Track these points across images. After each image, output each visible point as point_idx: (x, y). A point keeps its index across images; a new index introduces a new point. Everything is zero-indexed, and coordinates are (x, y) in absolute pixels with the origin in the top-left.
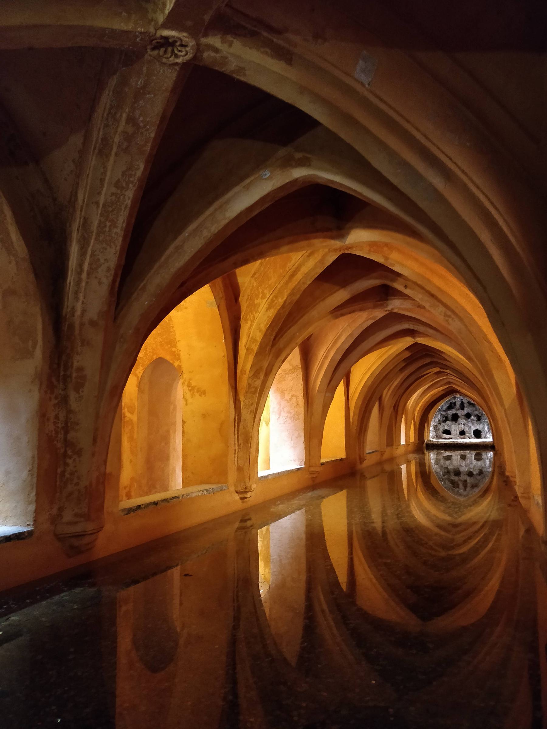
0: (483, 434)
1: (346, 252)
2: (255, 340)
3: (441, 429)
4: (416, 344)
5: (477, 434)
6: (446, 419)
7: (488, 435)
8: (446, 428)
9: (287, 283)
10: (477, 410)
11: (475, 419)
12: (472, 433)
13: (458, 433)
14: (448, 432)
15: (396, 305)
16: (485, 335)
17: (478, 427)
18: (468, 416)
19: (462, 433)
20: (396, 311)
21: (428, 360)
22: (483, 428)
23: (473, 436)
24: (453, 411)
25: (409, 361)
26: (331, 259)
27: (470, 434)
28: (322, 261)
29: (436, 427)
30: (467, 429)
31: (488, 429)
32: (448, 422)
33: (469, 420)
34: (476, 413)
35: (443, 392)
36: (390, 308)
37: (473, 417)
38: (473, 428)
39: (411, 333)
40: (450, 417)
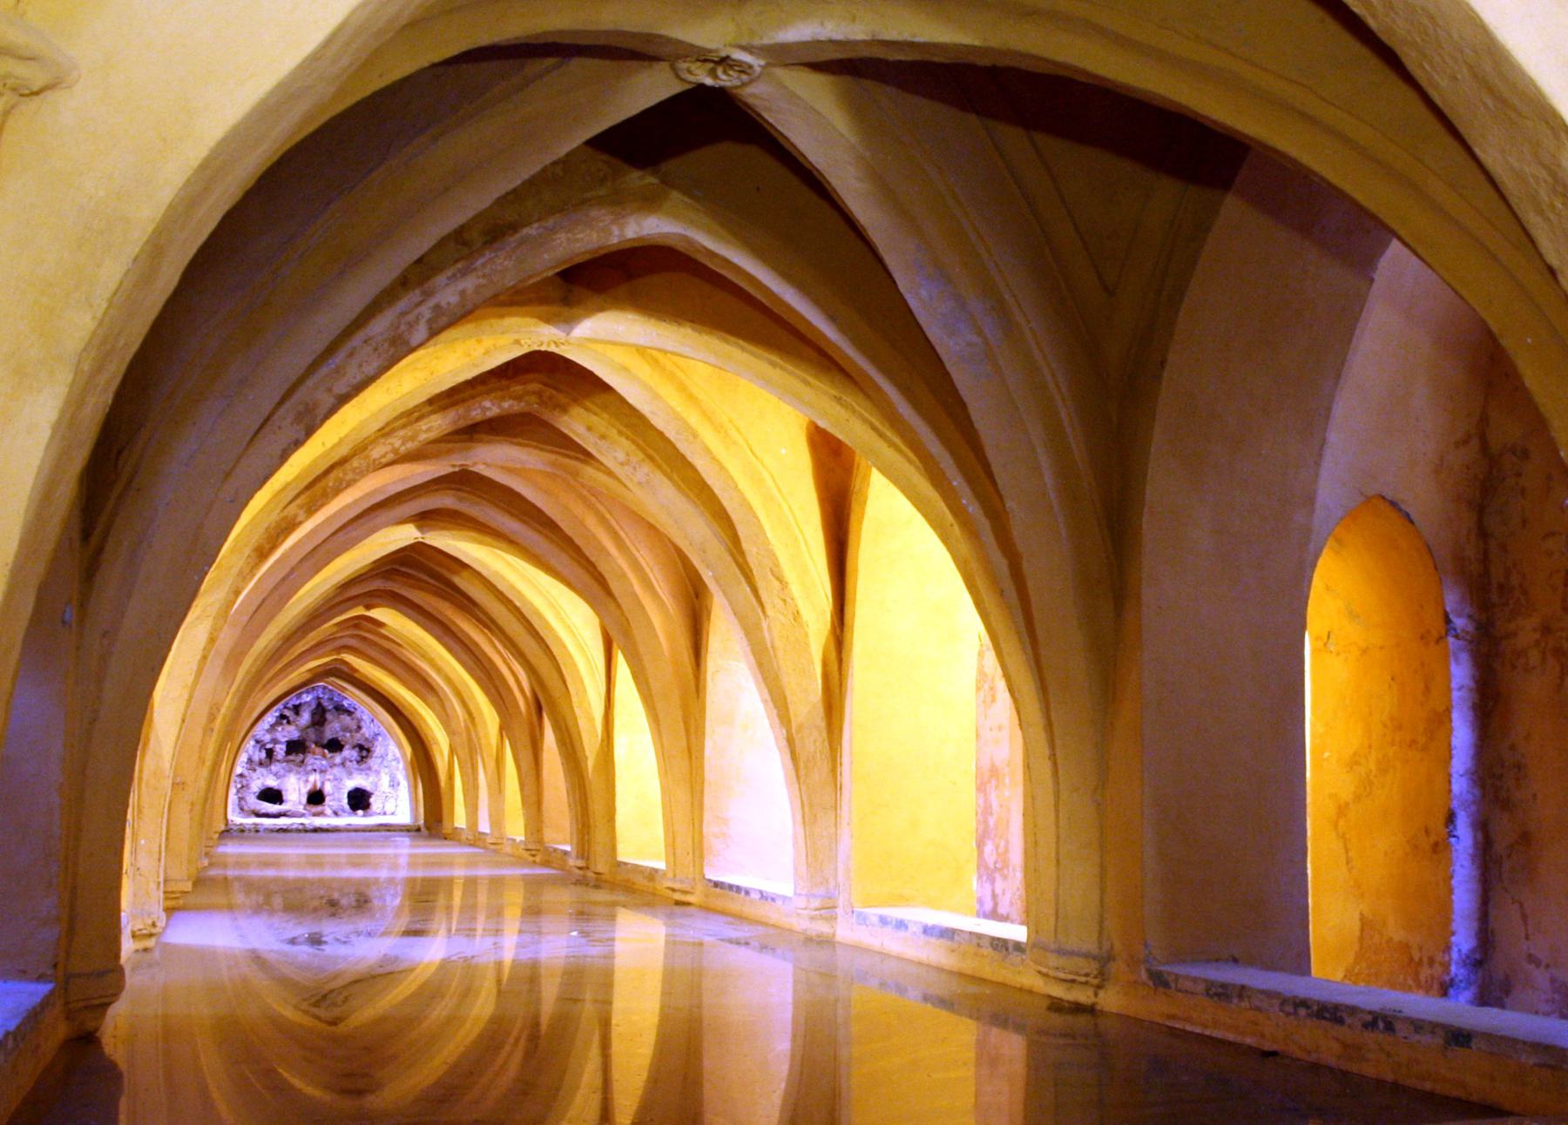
1: (553, 349)
3: (256, 785)
7: (389, 807)
8: (272, 782)
11: (355, 754)
12: (345, 801)
13: (304, 800)
16: (777, 565)
18: (335, 746)
20: (481, 469)
22: (376, 785)
23: (347, 807)
30: (328, 788)
31: (394, 784)
33: (338, 759)
35: (308, 676)
37: (349, 753)
38: (351, 784)
40: (280, 750)
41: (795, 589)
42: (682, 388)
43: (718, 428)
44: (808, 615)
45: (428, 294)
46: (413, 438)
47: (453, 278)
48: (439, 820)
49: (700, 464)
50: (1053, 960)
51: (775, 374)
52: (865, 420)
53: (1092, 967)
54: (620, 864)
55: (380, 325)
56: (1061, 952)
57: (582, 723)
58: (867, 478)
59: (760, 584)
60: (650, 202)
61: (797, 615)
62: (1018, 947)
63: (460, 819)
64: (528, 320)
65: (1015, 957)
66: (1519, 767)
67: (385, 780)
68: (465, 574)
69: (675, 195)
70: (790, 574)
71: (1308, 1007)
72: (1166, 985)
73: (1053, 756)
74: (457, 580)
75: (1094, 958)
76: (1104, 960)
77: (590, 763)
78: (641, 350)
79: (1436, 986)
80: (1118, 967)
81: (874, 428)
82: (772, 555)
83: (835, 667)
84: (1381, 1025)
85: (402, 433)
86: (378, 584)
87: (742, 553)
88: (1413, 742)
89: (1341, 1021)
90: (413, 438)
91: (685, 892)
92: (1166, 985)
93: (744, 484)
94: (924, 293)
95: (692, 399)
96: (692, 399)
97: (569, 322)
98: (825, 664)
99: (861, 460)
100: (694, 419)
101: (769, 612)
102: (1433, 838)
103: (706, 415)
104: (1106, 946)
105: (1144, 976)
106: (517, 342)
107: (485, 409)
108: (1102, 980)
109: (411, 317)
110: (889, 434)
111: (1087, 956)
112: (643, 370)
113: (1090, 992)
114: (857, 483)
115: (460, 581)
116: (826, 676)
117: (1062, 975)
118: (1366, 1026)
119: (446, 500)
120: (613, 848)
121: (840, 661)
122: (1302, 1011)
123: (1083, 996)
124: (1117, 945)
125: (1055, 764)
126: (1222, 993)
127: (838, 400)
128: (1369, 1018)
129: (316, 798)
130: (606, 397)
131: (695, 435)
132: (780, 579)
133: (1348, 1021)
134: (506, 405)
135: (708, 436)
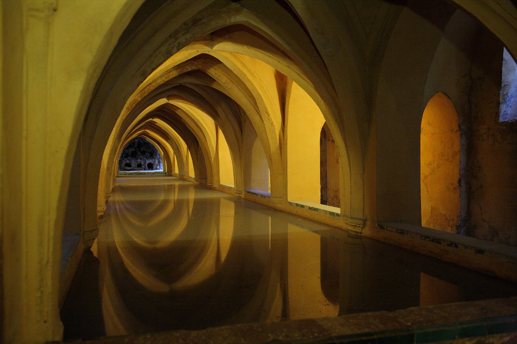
0: (155, 167)
1: (207, 53)
3: (124, 163)
5: (151, 166)
6: (127, 156)
7: (158, 167)
8: (128, 162)
10: (150, 148)
11: (149, 155)
14: (128, 165)
16: (267, 110)
17: (151, 161)
18: (143, 153)
19: (139, 166)
22: (154, 162)
24: (133, 150)
27: (145, 166)
29: (120, 162)
30: (143, 163)
32: (129, 158)
34: (149, 151)
37: (147, 154)
38: (148, 162)
41: (272, 116)
42: (242, 63)
44: (275, 123)
45: (177, 39)
46: (168, 77)
47: (183, 35)
48: (171, 171)
49: (246, 83)
50: (351, 220)
51: (270, 60)
52: (296, 72)
53: (361, 222)
54: (221, 185)
55: (163, 49)
56: (352, 218)
58: (291, 87)
60: (238, 12)
61: (272, 123)
62: (338, 215)
63: (177, 171)
64: (200, 45)
65: (336, 217)
67: (157, 161)
68: (179, 110)
69: (245, 10)
70: (270, 113)
71: (429, 238)
72: (384, 229)
73: (350, 164)
74: (177, 112)
75: (362, 220)
76: (365, 221)
77: (213, 159)
78: (231, 53)
79: (454, 227)
80: (368, 223)
81: (298, 74)
82: (266, 108)
83: (282, 137)
84: (454, 245)
85: (165, 76)
87: (258, 107)
88: (448, 160)
89: (440, 243)
90: (168, 77)
91: (239, 194)
92: (384, 229)
95: (245, 66)
96: (245, 66)
97: (212, 46)
98: (280, 136)
99: (289, 81)
100: (245, 71)
101: (265, 122)
102: (454, 186)
103: (249, 70)
104: (365, 217)
105: (377, 226)
106: (198, 51)
107: (187, 69)
108: (364, 224)
109: (172, 46)
110: (303, 76)
111: (360, 219)
112: (232, 59)
113: (360, 229)
114: (288, 88)
115: (178, 112)
117: (352, 224)
118: (448, 245)
120: (219, 181)
121: (284, 135)
122: (428, 239)
123: (358, 230)
124: (368, 217)
125: (350, 167)
126: (402, 232)
127: (288, 66)
128: (450, 243)
131: (245, 76)
132: (268, 114)
133: (443, 243)
134: (193, 68)
135: (249, 76)
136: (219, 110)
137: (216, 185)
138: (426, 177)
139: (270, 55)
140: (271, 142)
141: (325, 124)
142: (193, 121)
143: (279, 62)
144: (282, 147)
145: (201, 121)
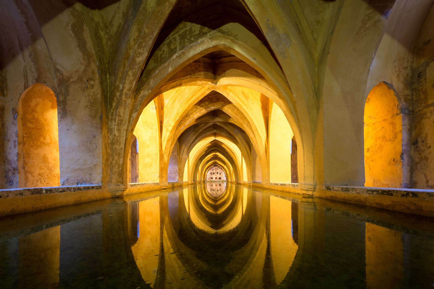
2: (171, 125)
4: (215, 140)
9: (187, 101)
15: (218, 120)
21: (214, 148)
25: (209, 148)
26: (208, 92)
28: (203, 94)
36: (214, 121)
39: (215, 135)
42: (238, 97)
43: (245, 105)
44: (262, 136)
49: (243, 111)
57: (239, 164)
59: (254, 132)
61: (260, 137)
66: (402, 141)
70: (259, 131)
86: (214, 148)
93: (250, 115)
94: (270, 35)
96: (240, 99)
100: (241, 103)
114: (270, 115)
115: (223, 146)
116: (265, 147)
119: (215, 131)
129: (216, 178)
130: (230, 105)
131: (241, 106)
132: (257, 131)
136: (237, 138)
137: (242, 182)
138: (368, 150)
139: (249, 80)
140: (260, 148)
141: (294, 136)
142: (229, 149)
143: (254, 83)
144: (267, 151)
145: (234, 149)
